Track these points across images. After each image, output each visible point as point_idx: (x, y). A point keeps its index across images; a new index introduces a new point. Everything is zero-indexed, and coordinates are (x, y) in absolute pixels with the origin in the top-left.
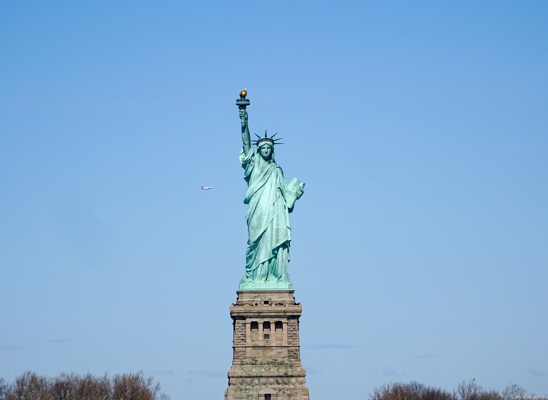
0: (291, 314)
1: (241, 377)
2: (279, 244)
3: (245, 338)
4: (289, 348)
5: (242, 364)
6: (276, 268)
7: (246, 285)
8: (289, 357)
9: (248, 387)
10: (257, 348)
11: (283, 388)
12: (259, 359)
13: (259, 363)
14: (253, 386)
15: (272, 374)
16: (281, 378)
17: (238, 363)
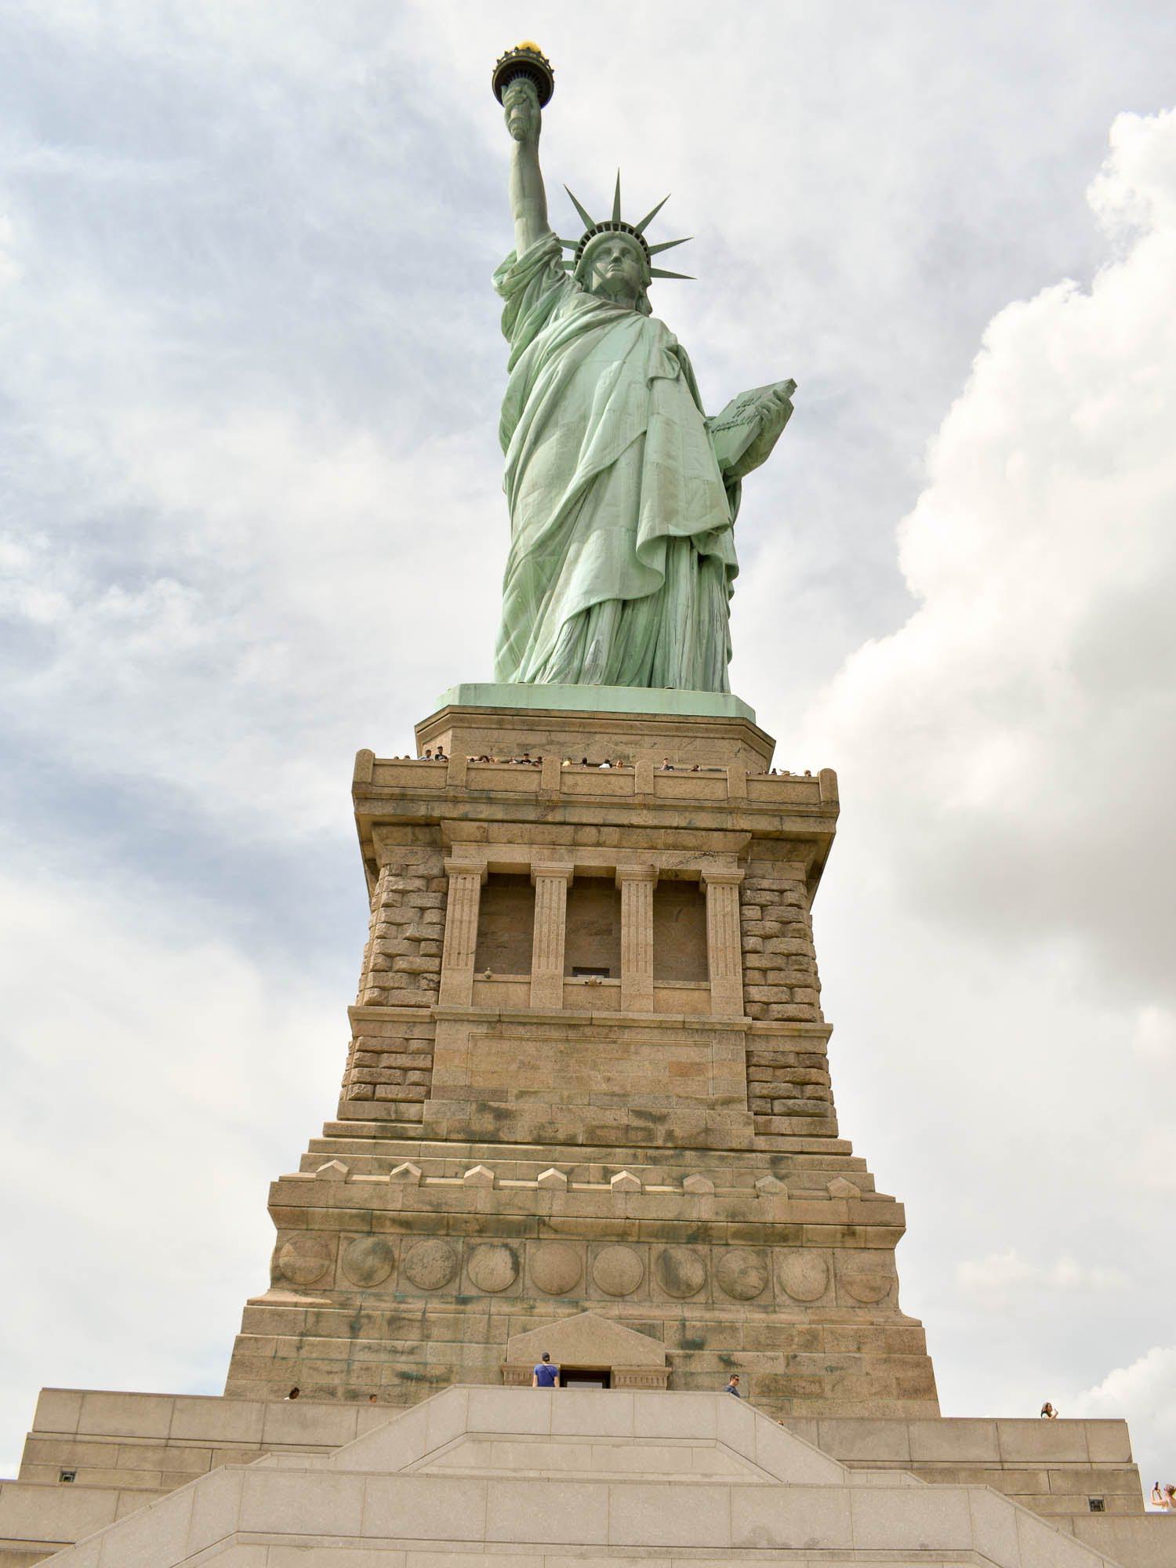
0: (764, 824)
1: (370, 1221)
2: (674, 531)
3: (437, 961)
4: (759, 1047)
5: (391, 1130)
6: (658, 662)
7: (473, 691)
8: (759, 1102)
9: (418, 1305)
10: (521, 1031)
11: (720, 1328)
12: (526, 1105)
13: (522, 1129)
14: (464, 1301)
15: (624, 1208)
16: (702, 1249)
17: (365, 1126)
